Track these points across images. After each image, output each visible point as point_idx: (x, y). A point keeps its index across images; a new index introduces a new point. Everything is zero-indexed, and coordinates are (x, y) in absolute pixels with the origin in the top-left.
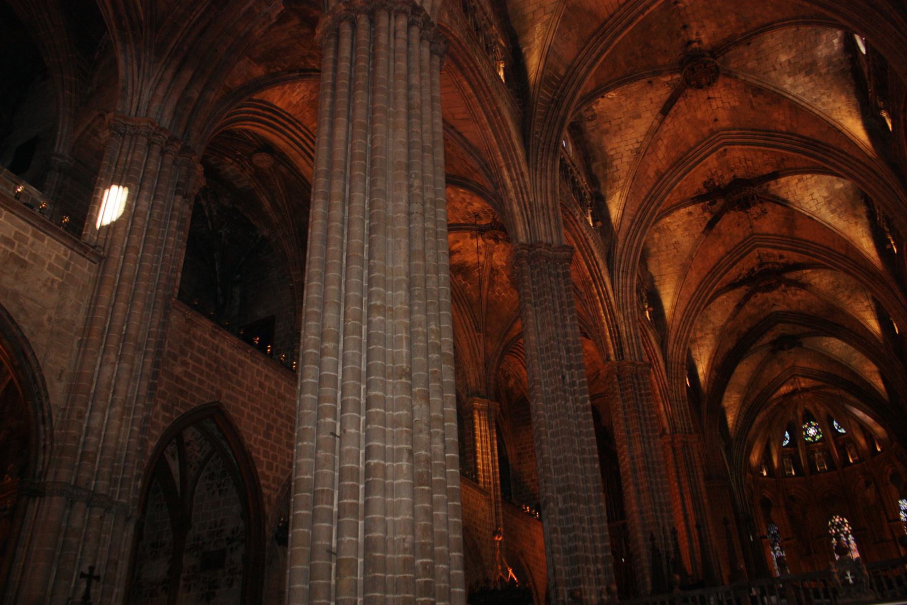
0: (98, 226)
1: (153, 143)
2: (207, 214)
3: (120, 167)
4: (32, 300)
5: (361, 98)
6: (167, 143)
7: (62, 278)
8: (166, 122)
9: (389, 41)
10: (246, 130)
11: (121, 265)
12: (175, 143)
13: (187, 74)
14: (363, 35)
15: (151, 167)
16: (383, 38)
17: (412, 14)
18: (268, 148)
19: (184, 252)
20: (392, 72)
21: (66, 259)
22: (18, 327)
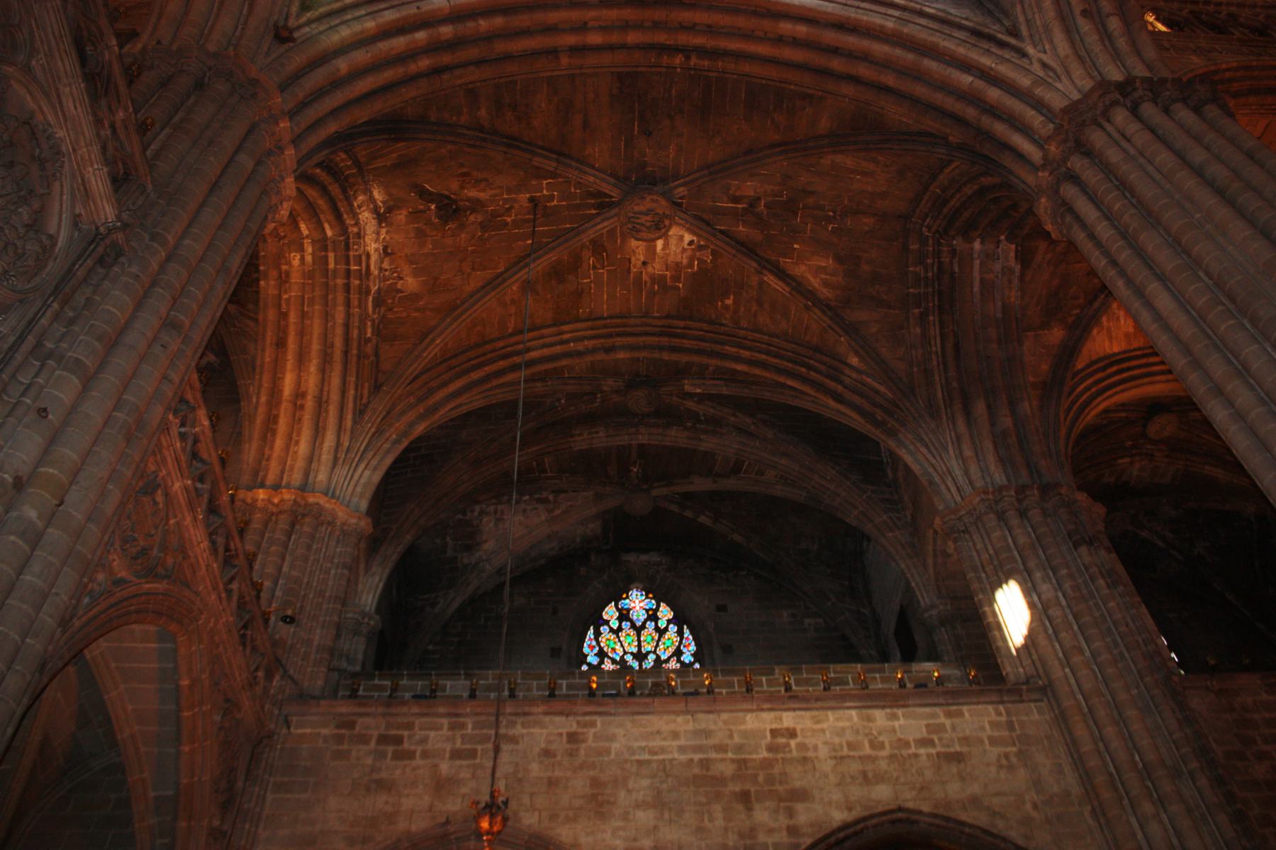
0: (1014, 652)
1: (1004, 512)
2: (1160, 544)
3: (989, 568)
4: (998, 794)
5: (1151, 241)
6: (1019, 501)
7: (1014, 744)
8: (999, 478)
9: (1123, 150)
10: (1106, 411)
11: (1073, 681)
12: (1028, 493)
13: (980, 408)
14: (1091, 176)
15: (1022, 540)
16: (1114, 156)
17: (1125, 97)
18: (1154, 407)
19: (1144, 609)
20: (1158, 177)
21: (1004, 719)
22: (1004, 839)
